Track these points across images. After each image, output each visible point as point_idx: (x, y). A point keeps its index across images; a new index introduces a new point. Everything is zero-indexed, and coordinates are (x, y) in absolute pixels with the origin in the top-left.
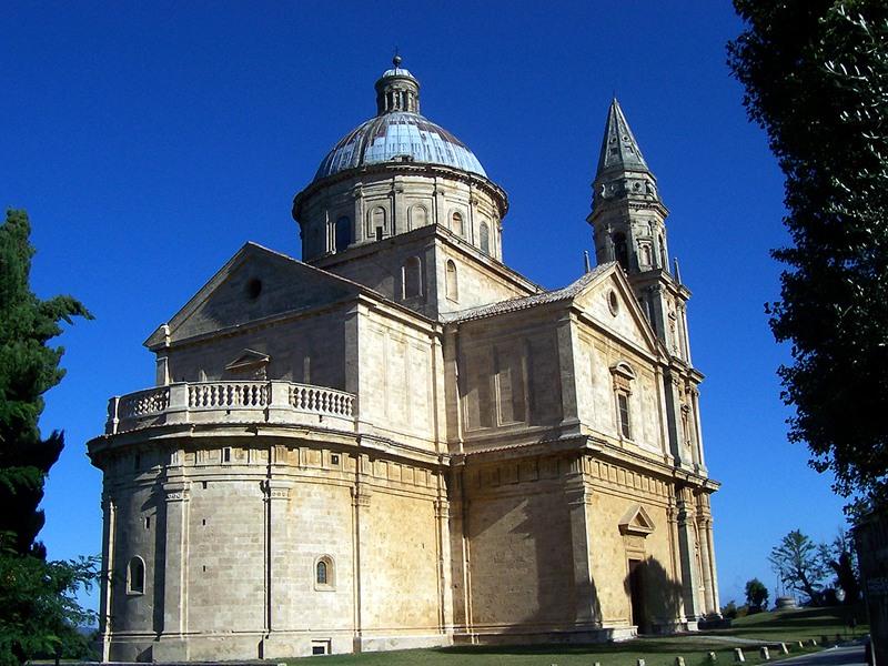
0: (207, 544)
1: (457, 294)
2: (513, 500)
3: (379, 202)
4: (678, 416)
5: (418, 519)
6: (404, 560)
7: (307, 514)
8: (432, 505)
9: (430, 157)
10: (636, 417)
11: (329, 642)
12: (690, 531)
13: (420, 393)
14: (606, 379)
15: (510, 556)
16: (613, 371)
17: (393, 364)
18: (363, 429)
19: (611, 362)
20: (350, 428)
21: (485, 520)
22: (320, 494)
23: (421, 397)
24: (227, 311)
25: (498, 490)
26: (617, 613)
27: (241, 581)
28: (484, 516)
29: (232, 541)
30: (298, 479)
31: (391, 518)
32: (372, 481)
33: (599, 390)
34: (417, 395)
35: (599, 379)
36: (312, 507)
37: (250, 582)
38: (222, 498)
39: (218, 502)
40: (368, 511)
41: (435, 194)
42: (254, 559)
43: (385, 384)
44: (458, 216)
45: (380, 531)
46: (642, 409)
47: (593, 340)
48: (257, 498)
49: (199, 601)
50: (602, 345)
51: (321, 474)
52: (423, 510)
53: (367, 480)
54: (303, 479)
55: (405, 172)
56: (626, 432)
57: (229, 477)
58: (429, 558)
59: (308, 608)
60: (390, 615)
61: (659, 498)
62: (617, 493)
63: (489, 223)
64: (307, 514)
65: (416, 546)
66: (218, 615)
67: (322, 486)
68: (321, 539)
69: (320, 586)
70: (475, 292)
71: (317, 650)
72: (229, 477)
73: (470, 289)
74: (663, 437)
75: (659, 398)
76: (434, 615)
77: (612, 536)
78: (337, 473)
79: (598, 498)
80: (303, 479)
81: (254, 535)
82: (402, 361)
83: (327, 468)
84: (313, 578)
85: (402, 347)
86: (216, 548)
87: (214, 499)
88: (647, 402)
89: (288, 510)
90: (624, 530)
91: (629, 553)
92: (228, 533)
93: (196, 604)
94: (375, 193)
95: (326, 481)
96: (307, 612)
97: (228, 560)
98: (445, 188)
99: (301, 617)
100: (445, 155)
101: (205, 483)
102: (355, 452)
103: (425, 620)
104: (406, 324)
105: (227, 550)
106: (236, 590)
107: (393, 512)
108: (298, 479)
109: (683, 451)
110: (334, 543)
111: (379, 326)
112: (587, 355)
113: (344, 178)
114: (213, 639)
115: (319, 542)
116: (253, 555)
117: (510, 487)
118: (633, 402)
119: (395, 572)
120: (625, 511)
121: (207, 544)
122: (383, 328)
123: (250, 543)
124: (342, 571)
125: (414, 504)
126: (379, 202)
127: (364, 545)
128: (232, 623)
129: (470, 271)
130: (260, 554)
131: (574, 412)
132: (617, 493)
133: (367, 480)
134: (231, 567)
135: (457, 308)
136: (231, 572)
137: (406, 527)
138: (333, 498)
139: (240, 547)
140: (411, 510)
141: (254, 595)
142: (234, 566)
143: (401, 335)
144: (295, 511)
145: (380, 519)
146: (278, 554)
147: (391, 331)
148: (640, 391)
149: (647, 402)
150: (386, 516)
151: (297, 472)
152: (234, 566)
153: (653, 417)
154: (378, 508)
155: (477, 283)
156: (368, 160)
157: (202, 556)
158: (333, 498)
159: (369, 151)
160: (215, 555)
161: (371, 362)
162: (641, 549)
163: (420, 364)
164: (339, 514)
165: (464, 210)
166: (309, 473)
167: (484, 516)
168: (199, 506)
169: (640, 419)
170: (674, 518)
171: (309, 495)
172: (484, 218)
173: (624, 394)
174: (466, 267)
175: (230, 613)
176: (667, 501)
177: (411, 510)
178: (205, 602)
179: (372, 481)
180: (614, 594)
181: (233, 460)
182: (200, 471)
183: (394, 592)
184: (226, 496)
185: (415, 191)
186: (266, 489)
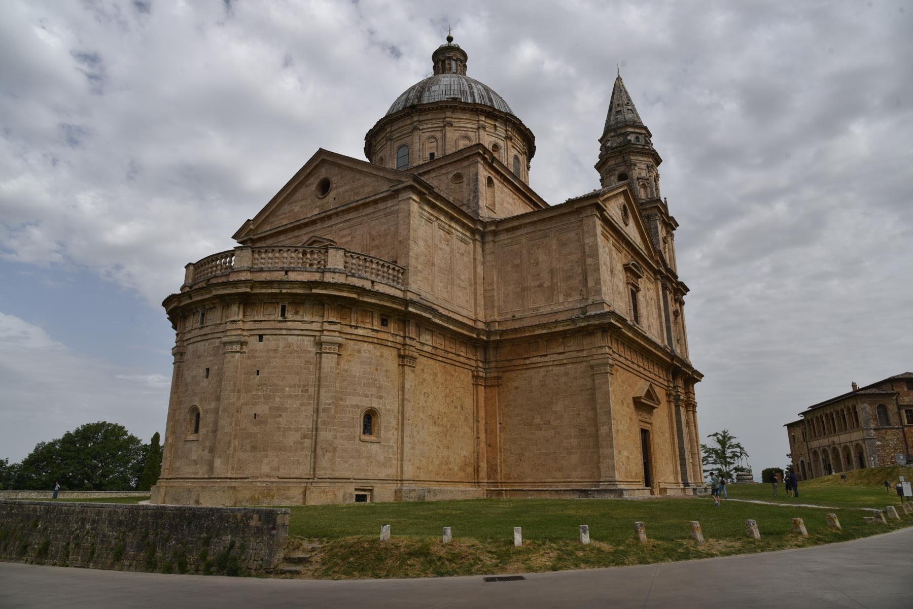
0: (260, 393)
1: (494, 205)
2: (541, 370)
3: (433, 134)
4: (672, 318)
5: (458, 385)
6: (445, 419)
7: (356, 368)
8: (471, 373)
9: (474, 100)
10: (643, 310)
11: (371, 491)
12: (682, 410)
13: (463, 277)
14: (621, 275)
15: (539, 420)
16: (627, 268)
17: (441, 249)
18: (409, 296)
19: (625, 262)
20: (399, 294)
21: (517, 388)
22: (369, 352)
23: (463, 281)
24: (301, 207)
25: (528, 362)
26: (634, 474)
27: (289, 429)
28: (516, 384)
29: (283, 390)
30: (349, 337)
31: (434, 380)
32: (418, 346)
33: (616, 281)
34: (460, 278)
35: (616, 272)
36: (362, 363)
37: (297, 430)
38: (276, 350)
39: (271, 354)
40: (413, 371)
41: (478, 128)
42: (303, 408)
43: (433, 264)
44: (496, 147)
45: (425, 390)
46: (647, 306)
47: (611, 238)
48: (310, 352)
49: (248, 447)
50: (618, 245)
51: (371, 334)
52: (462, 376)
53: (414, 343)
54: (353, 337)
55: (454, 109)
56: (636, 318)
57: (284, 332)
58: (466, 419)
59: (353, 457)
60: (431, 468)
61: (661, 381)
62: (631, 370)
63: (520, 157)
64: (356, 368)
65: (456, 408)
66: (266, 461)
67: (371, 346)
68: (369, 393)
69: (367, 437)
70: (509, 207)
71: (360, 498)
72: (284, 332)
73: (505, 205)
74: (662, 331)
75: (658, 299)
76: (470, 470)
77: (628, 407)
78: (386, 334)
79: (617, 371)
80: (353, 337)
81: (304, 386)
82: (448, 249)
83: (377, 329)
84: (359, 429)
85: (448, 236)
86: (267, 397)
87: (268, 351)
88: (650, 301)
89: (338, 364)
90: (637, 402)
91: (641, 424)
92: (281, 384)
93: (245, 451)
94: (429, 126)
95: (375, 341)
96: (351, 461)
97: (278, 409)
98: (486, 124)
99: (346, 465)
100: (487, 100)
101: (261, 338)
102: (404, 319)
103: (462, 474)
104: (452, 218)
105: (277, 399)
106: (284, 436)
107: (436, 375)
108: (349, 337)
109: (676, 346)
110: (381, 397)
111: (429, 215)
112: (607, 250)
113: (405, 115)
114: (259, 484)
115: (367, 396)
116: (302, 404)
117: (539, 359)
118: (640, 296)
119: (436, 429)
120: (640, 389)
121: (260, 393)
122: (432, 217)
123: (300, 393)
124: (387, 423)
125: (455, 371)
126: (433, 134)
127: (409, 401)
128: (278, 469)
129: (506, 189)
130: (311, 403)
131: (598, 292)
132: (631, 370)
133: (414, 343)
134: (280, 415)
135: (494, 216)
136: (281, 419)
137: (448, 390)
138: (382, 356)
139: (290, 396)
140: (453, 376)
141: (301, 443)
142: (284, 414)
143: (447, 227)
144: (344, 365)
145: (425, 380)
146: (326, 404)
147: (439, 221)
148: (645, 290)
149: (650, 301)
150: (429, 378)
151: (349, 330)
152: (284, 414)
153: (654, 313)
154: (423, 370)
155: (511, 201)
156: (425, 101)
157: (255, 404)
158: (382, 356)
159: (426, 94)
160: (265, 404)
161: (421, 243)
162: (649, 421)
163: (463, 254)
164: (387, 371)
165: (501, 143)
166: (360, 332)
167: (516, 384)
168: (254, 357)
169: (645, 312)
170: (672, 398)
171: (359, 352)
172: (516, 153)
173: (635, 290)
174: (502, 186)
175: (276, 459)
176: (666, 383)
177: (453, 376)
178: (254, 448)
179: (418, 346)
180: (630, 457)
181: (289, 316)
182: (258, 326)
183: (435, 447)
184: (280, 349)
185: (462, 125)
186: (320, 344)
